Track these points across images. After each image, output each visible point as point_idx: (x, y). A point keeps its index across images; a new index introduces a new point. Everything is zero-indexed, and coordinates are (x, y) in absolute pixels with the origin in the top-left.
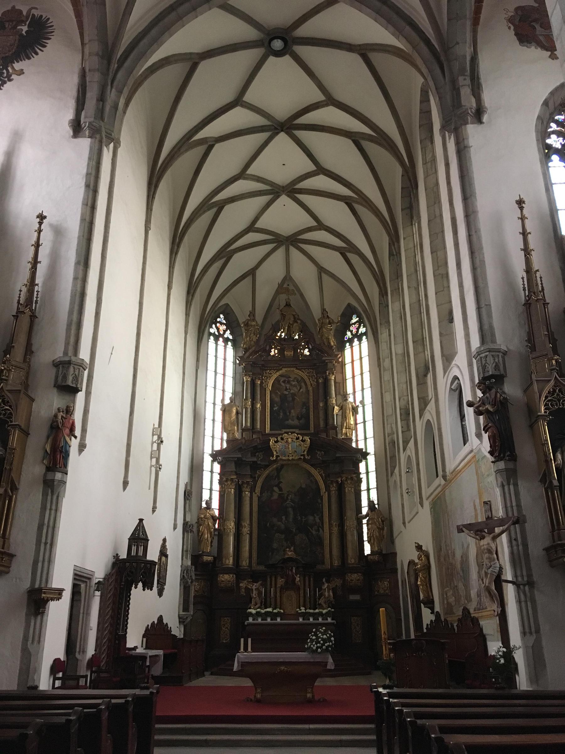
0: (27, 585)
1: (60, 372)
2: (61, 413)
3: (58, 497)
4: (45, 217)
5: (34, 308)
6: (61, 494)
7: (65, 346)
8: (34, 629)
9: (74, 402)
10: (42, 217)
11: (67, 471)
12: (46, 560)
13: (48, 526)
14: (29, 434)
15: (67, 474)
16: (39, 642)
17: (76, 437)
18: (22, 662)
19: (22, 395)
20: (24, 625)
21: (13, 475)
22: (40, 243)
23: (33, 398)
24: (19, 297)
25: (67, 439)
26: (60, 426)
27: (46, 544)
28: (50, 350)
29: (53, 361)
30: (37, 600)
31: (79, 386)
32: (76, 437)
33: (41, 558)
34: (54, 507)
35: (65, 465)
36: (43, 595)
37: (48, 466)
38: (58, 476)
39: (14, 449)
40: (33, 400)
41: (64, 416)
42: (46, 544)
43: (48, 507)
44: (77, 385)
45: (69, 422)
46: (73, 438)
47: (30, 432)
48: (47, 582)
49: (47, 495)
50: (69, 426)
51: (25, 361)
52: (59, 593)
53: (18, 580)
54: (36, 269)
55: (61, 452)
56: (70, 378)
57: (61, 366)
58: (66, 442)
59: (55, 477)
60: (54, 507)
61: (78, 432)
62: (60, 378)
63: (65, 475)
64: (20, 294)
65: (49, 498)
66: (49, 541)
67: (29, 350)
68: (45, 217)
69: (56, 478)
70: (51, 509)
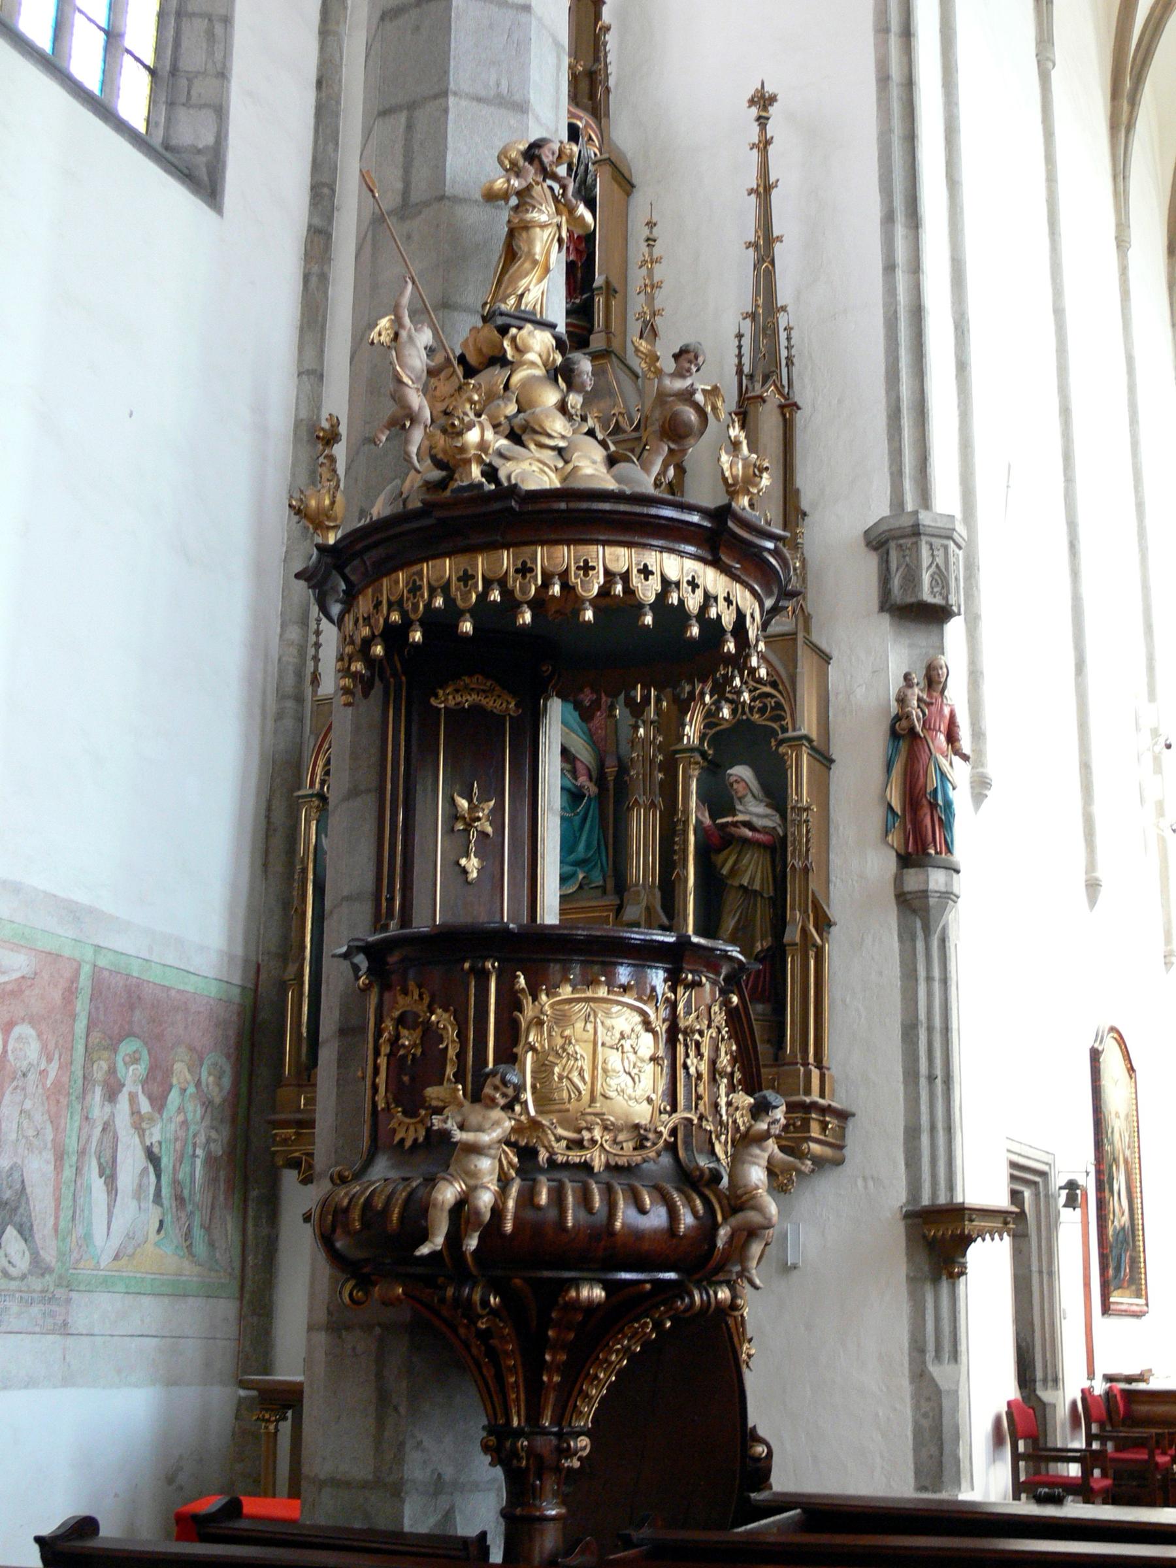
0: (897, 1196)
1: (893, 566)
3: (943, 941)
8: (937, 1319)
12: (940, 1125)
13: (930, 1029)
16: (955, 1356)
18: (916, 1407)
25: (944, 763)
26: (919, 728)
27: (931, 1078)
28: (844, 504)
32: (965, 758)
34: (936, 973)
37: (902, 852)
38: (937, 879)
42: (931, 1078)
46: (956, 760)
48: (951, 1188)
49: (913, 939)
53: (870, 1184)
55: (933, 806)
56: (926, 578)
57: (892, 544)
60: (936, 973)
63: (955, 875)
65: (920, 945)
66: (939, 1072)
69: (932, 886)
70: (929, 979)
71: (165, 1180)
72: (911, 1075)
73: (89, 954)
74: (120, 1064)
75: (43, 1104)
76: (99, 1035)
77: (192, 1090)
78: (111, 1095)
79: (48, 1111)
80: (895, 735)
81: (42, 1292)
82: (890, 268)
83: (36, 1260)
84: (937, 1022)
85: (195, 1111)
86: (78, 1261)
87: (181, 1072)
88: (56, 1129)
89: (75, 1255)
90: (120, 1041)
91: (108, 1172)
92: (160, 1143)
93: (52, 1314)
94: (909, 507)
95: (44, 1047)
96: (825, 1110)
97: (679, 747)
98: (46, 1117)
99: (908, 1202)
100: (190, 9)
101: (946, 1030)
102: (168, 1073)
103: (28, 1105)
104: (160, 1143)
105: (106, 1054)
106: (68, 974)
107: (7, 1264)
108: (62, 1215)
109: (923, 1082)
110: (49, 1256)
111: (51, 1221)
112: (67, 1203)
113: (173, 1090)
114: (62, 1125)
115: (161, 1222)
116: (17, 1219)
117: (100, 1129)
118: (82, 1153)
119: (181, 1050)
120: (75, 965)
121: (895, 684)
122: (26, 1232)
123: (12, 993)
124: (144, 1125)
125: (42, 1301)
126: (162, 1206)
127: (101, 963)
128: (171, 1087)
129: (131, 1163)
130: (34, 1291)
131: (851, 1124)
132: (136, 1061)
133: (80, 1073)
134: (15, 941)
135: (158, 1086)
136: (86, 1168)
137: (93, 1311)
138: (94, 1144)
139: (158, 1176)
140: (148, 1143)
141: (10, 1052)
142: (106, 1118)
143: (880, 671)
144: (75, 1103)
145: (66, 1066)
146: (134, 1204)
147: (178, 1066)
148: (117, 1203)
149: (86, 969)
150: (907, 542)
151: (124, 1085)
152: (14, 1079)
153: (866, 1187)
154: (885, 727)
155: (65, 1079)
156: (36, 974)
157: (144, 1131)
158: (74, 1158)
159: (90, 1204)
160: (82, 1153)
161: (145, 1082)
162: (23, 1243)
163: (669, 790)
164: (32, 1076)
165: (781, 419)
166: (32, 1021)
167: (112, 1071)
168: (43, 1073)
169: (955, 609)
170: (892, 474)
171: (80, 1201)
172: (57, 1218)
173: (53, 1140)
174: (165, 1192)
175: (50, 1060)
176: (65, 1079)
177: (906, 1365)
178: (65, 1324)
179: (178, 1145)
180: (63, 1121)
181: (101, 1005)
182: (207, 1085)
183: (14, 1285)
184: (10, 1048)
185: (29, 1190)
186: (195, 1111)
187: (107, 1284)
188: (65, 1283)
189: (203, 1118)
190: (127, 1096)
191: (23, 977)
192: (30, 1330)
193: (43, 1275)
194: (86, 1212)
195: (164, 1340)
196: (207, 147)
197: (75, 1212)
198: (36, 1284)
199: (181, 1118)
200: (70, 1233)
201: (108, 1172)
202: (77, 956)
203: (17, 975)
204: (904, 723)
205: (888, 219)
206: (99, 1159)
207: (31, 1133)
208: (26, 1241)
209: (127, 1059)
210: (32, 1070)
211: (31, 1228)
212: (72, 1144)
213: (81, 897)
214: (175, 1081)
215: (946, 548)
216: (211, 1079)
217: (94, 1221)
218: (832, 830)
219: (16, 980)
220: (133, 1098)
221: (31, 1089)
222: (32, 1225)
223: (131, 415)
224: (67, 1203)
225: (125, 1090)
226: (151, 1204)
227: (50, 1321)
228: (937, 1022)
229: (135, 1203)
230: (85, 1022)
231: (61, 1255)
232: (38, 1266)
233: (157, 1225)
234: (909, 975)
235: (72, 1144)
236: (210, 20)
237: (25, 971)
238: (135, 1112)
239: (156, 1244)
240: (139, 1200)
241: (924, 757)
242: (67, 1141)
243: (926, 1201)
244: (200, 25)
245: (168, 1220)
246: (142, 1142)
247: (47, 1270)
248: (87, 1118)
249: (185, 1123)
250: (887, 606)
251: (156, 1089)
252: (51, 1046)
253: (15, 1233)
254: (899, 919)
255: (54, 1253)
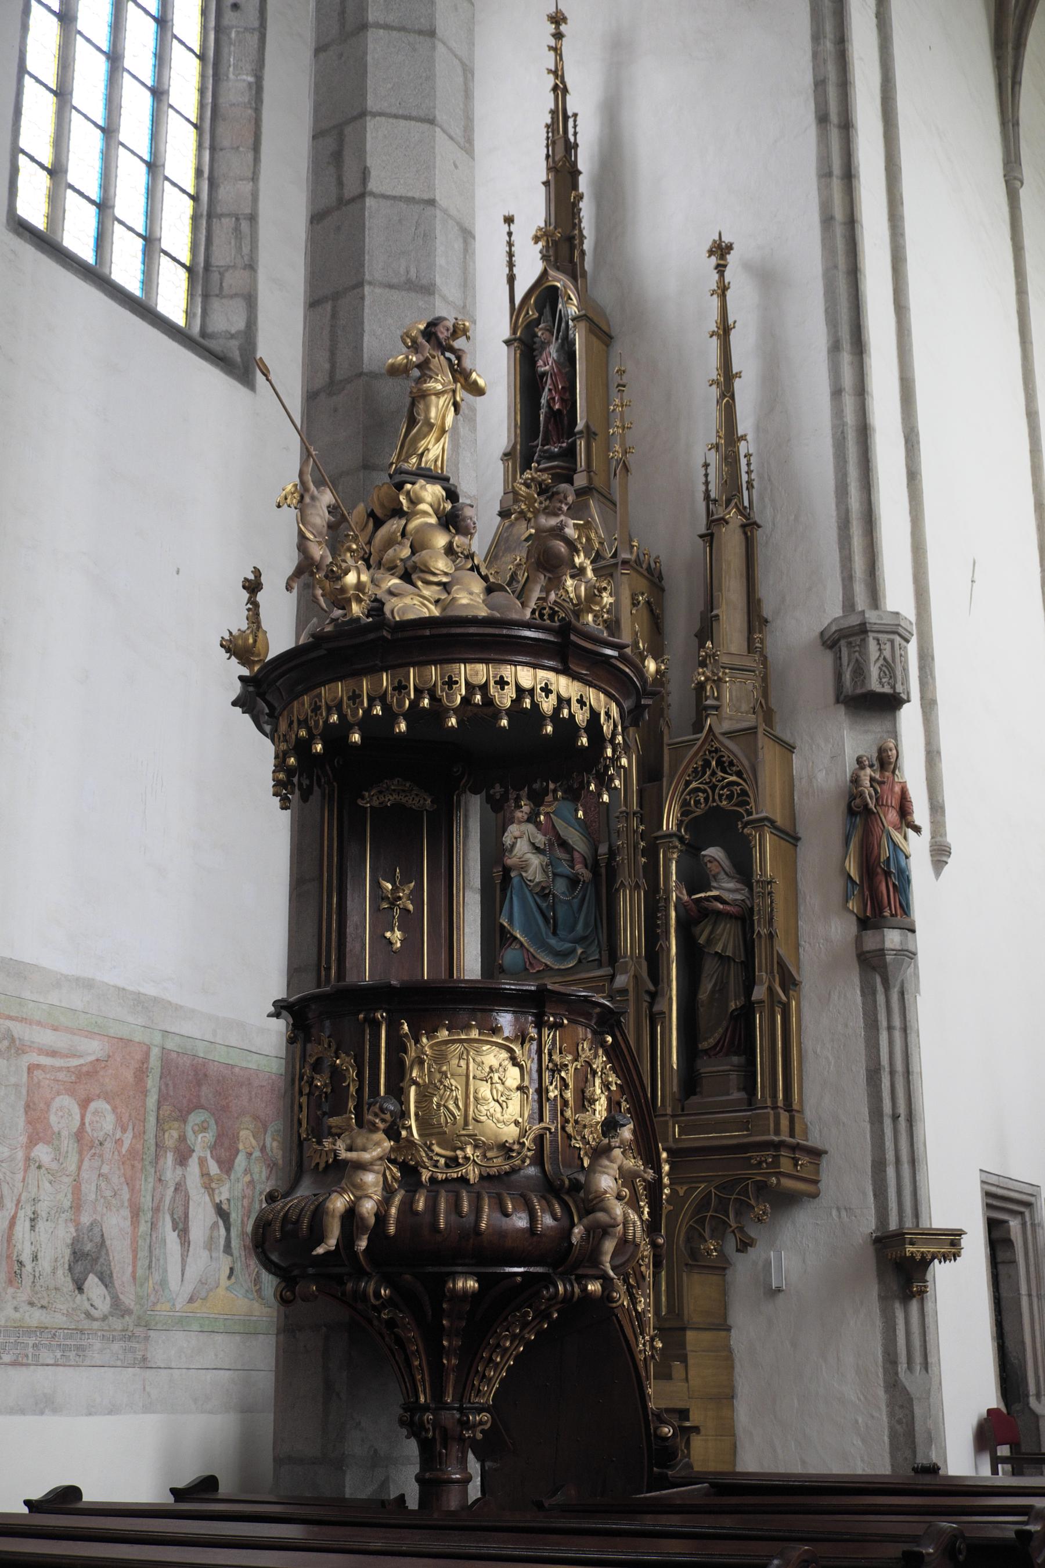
0: (868, 1224)
2: (868, 771)
3: (902, 994)
4: (729, 247)
5: (746, 504)
6: (909, 987)
7: (844, 587)
9: (895, 734)
10: (721, 250)
11: (913, 923)
13: (892, 1073)
14: (798, 839)
15: (913, 931)
16: (926, 1366)
17: (917, 830)
18: (891, 1414)
19: (762, 740)
20: (879, 1323)
21: (781, 948)
22: (731, 322)
23: (791, 742)
24: (707, 483)
25: (897, 837)
26: (872, 806)
27: (895, 1117)
29: (822, 633)
30: (902, 1264)
31: (899, 688)
32: (917, 830)
33: (890, 1156)
34: (897, 1022)
35: (905, 909)
36: (910, 1249)
37: (861, 916)
38: (893, 938)
39: (769, 883)
40: (790, 748)
41: (877, 776)
42: (895, 1117)
43: (883, 1023)
44: (894, 687)
45: (892, 789)
46: (911, 833)
47: (801, 832)
48: (916, 1215)
49: (874, 993)
50: (895, 802)
51: (751, 648)
52: (951, 1243)
53: (844, 1214)
54: (733, 397)
55: (887, 874)
56: (874, 671)
57: (843, 642)
58: (896, 845)
59: (883, 942)
60: (897, 1022)
61: (921, 814)
62: (847, 676)
63: (909, 934)
64: (706, 475)
65: (881, 998)
66: (902, 1110)
67: (756, 619)
68: (729, 247)
69: (888, 945)
70: (890, 1028)
71: (234, 1233)
72: (876, 1114)
73: (157, 1039)
74: (190, 1134)
75: (119, 1169)
76: (169, 1108)
77: (257, 1154)
78: (182, 1158)
79: (124, 1175)
80: (851, 812)
81: (123, 1330)
82: (837, 393)
83: (116, 1302)
84: (899, 1066)
85: (261, 1172)
86: (154, 1304)
87: (247, 1139)
88: (132, 1190)
89: (152, 1298)
90: (189, 1112)
91: (181, 1226)
92: (228, 1200)
93: (133, 1350)
94: (860, 607)
95: (119, 1118)
96: (795, 1148)
97: (659, 833)
98: (122, 1179)
99: (877, 1229)
100: (219, 210)
101: (907, 1072)
102: (235, 1138)
103: (105, 1169)
104: (228, 1200)
105: (176, 1124)
106: (139, 1056)
107: (89, 1307)
108: (139, 1264)
109: (888, 1122)
110: (128, 1299)
111: (130, 1269)
112: (143, 1254)
113: (240, 1154)
114: (138, 1187)
115: (232, 1269)
116: (98, 1268)
117: (172, 1189)
118: (156, 1210)
119: (247, 1119)
120: (145, 1048)
121: (850, 765)
122: (106, 1280)
123: (88, 1073)
124: (213, 1185)
125: (123, 1338)
126: (232, 1255)
127: (170, 1045)
128: (238, 1151)
129: (202, 1218)
130: (115, 1330)
131: (824, 1161)
132: (204, 1129)
133: (153, 1142)
134: (89, 1029)
135: (225, 1152)
136: (160, 1224)
137: (169, 1347)
138: (167, 1202)
139: (228, 1230)
140: (218, 1201)
141: (87, 1124)
142: (177, 1180)
143: (837, 756)
144: (148, 1168)
145: (139, 1135)
146: (205, 1254)
147: (243, 1134)
148: (190, 1253)
149: (155, 1052)
150: (857, 640)
151: (193, 1151)
152: (91, 1148)
153: (840, 1217)
154: (843, 806)
155: (139, 1146)
156: (109, 1056)
157: (213, 1190)
158: (149, 1215)
159: (165, 1254)
160: (156, 1210)
161: (213, 1148)
162: (103, 1287)
163: (651, 871)
164: (108, 1145)
165: (743, 537)
166: (107, 1097)
167: (183, 1138)
168: (119, 1142)
169: (904, 697)
170: (843, 580)
171: (156, 1252)
172: (134, 1266)
173: (130, 1200)
174: (235, 1243)
175: (124, 1130)
176: (139, 1146)
177: (881, 1375)
178: (144, 1359)
179: (246, 1202)
180: (138, 1182)
181: (170, 1083)
182: (272, 1150)
183: (96, 1325)
184: (87, 1121)
185: (108, 1243)
186: (261, 1172)
187: (181, 1323)
188: (143, 1323)
189: (268, 1179)
190: (196, 1160)
191: (97, 1060)
192: (112, 1363)
193: (123, 1316)
194: (162, 1262)
195: (237, 1372)
196: (239, 332)
197: (151, 1262)
198: (117, 1324)
199: (247, 1178)
200: (147, 1279)
201: (181, 1226)
202: (147, 1042)
203: (93, 1058)
204: (858, 801)
205: (835, 348)
206: (172, 1215)
207: (108, 1193)
208: (106, 1286)
209: (196, 1128)
210: (108, 1139)
211: (111, 1276)
212: (147, 1202)
213: (150, 990)
214: (241, 1147)
215: (892, 642)
216: (275, 1144)
217: (169, 1269)
218: (800, 901)
219: (91, 1062)
220: (202, 1162)
221: (108, 1156)
222: (111, 1273)
223: (178, 573)
224: (143, 1254)
225: (195, 1156)
226: (221, 1254)
227: (130, 1355)
228: (899, 1066)
229: (207, 1252)
230: (156, 1097)
231: (139, 1298)
232: (118, 1308)
233: (228, 1272)
234: (872, 1025)
235: (147, 1202)
236: (237, 219)
237: (100, 1055)
238: (205, 1174)
239: (227, 1289)
240: (210, 1250)
241: (878, 830)
242: (143, 1199)
243: (893, 1225)
244: (228, 223)
245: (238, 1267)
246: (212, 1199)
247: (128, 1312)
248: (160, 1180)
249: (252, 1182)
250: (842, 698)
251: (224, 1154)
252: (125, 1119)
253: (96, 1280)
254: (861, 975)
255: (132, 1297)
